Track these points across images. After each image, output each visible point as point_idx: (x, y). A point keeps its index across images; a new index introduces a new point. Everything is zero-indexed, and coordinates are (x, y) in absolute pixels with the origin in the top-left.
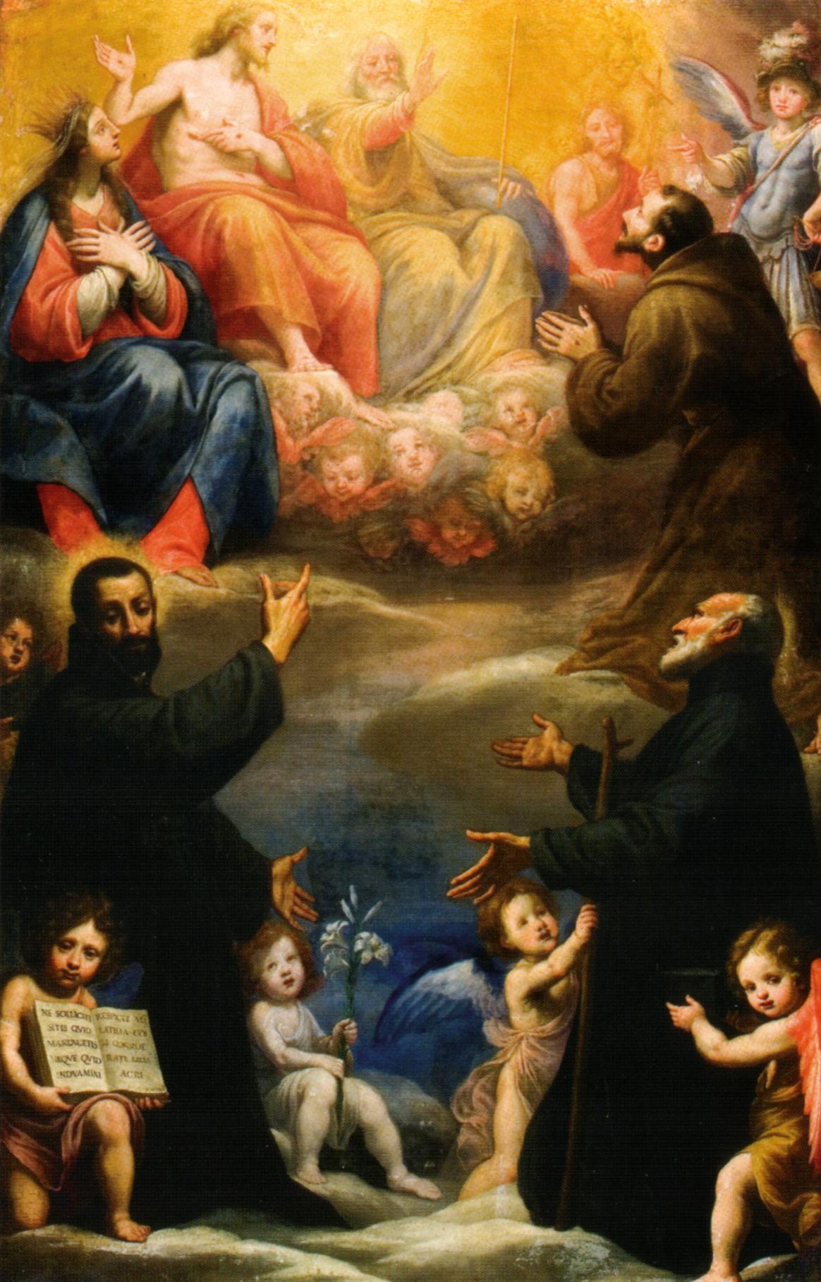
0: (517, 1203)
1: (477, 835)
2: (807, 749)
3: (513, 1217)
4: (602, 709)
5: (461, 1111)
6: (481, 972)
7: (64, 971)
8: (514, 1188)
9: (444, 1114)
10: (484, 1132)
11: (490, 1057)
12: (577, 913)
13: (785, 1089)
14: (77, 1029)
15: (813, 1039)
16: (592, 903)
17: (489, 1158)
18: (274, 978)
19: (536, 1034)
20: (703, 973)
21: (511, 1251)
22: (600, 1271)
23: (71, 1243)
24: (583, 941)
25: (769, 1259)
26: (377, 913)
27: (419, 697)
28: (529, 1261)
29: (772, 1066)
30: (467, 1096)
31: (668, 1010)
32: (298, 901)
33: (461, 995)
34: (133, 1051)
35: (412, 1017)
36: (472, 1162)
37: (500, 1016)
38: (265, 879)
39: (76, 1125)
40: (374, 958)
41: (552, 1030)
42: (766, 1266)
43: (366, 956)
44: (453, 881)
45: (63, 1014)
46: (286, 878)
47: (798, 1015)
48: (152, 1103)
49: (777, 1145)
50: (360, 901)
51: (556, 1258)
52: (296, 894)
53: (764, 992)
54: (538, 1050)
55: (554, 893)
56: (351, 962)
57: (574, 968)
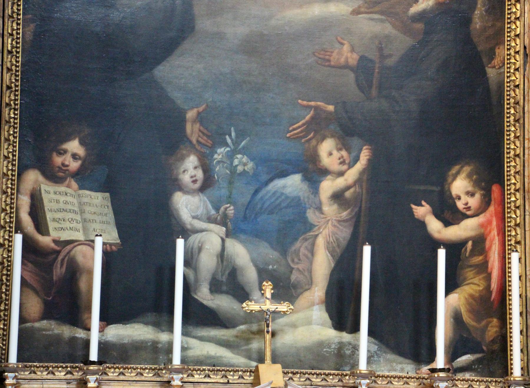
0: (325, 316)
1: (305, 103)
2: (489, 65)
3: (323, 325)
4: (375, 37)
5: (293, 261)
6: (306, 181)
7: (59, 167)
8: (323, 307)
9: (283, 262)
10: (306, 274)
11: (310, 230)
12: (361, 150)
13: (478, 257)
14: (66, 203)
16: (369, 146)
17: (309, 289)
18: (186, 178)
20: (435, 188)
21: (321, 344)
22: (372, 358)
23: (56, 332)
24: (364, 167)
25: (469, 355)
27: (273, 22)
28: (331, 351)
29: (470, 243)
31: (411, 209)
33: (295, 194)
34: (100, 217)
35: (266, 205)
36: (299, 291)
37: (316, 207)
38: (184, 120)
39: (63, 260)
40: (244, 170)
41: (346, 217)
42: (467, 360)
43: (240, 169)
44: (291, 129)
45: (58, 193)
46: (194, 122)
47: (485, 215)
48: (111, 248)
49: (472, 289)
50: (237, 137)
51: (347, 350)
52: (200, 130)
53: (466, 202)
54: (338, 227)
55: (347, 138)
56: (231, 172)
57: (358, 181)
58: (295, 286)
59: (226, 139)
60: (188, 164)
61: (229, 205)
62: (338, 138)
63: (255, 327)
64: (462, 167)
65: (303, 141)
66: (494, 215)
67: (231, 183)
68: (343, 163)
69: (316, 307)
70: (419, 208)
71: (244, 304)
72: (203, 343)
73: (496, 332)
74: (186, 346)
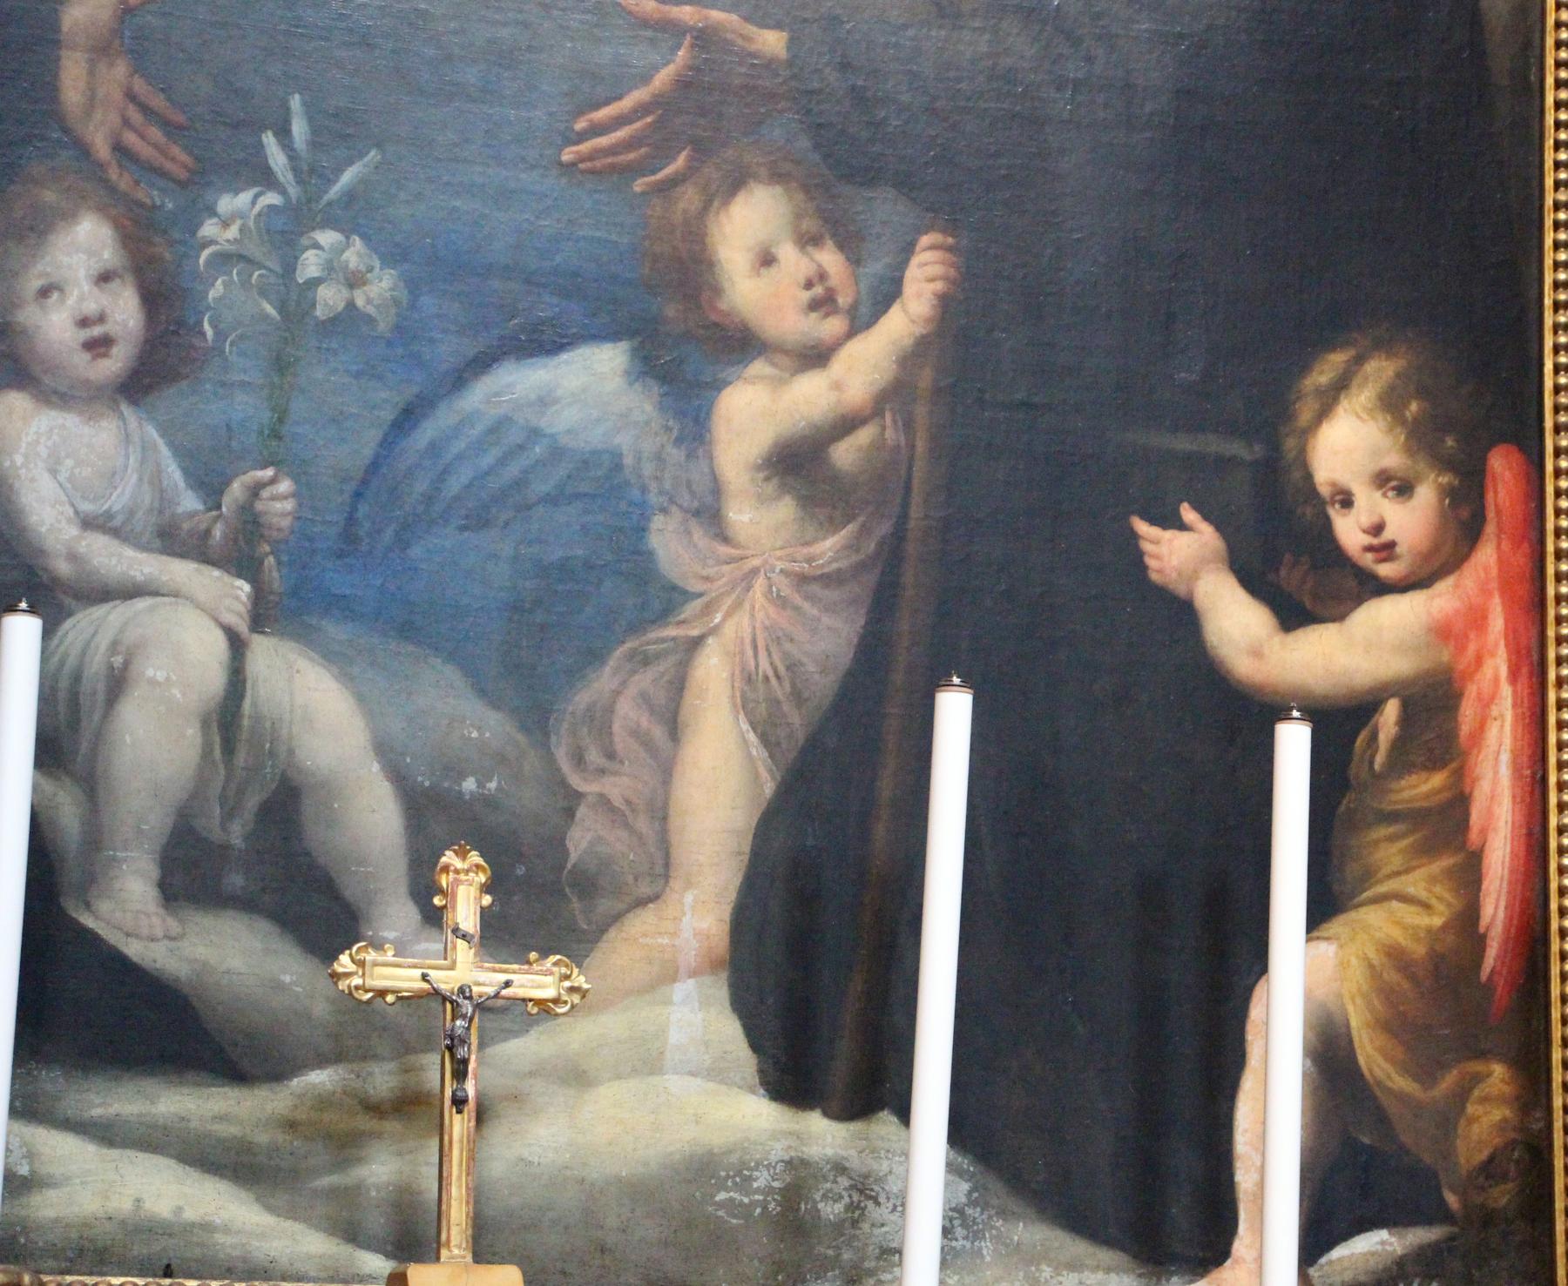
0: (729, 1032)
3: (716, 1073)
5: (579, 759)
6: (650, 382)
8: (719, 990)
9: (532, 763)
10: (642, 824)
11: (665, 614)
12: (908, 250)
13: (1424, 775)
15: (1493, 655)
16: (944, 232)
19: (796, 567)
20: (1236, 448)
24: (919, 330)
25: (1383, 1234)
26: (363, 181)
28: (753, 1204)
29: (1391, 712)
30: (600, 720)
31: (1134, 536)
32: (136, 117)
33: (595, 438)
35: (454, 485)
36: (605, 905)
37: (696, 504)
40: (351, 305)
41: (834, 560)
42: (1373, 1254)
43: (330, 298)
44: (580, 125)
47: (1456, 586)
50: (314, 145)
51: (825, 1197)
52: (131, 96)
53: (1375, 519)
54: (797, 609)
55: (847, 189)
56: (282, 308)
58: (587, 884)
59: (260, 147)
60: (66, 260)
61: (269, 472)
62: (806, 189)
63: (382, 1080)
64: (1359, 360)
65: (639, 185)
66: (1494, 585)
67: (281, 364)
68: (823, 304)
69: (685, 989)
70: (1168, 535)
71: (344, 958)
72: (115, 1153)
73: (1502, 1126)
74: (24, 1170)
